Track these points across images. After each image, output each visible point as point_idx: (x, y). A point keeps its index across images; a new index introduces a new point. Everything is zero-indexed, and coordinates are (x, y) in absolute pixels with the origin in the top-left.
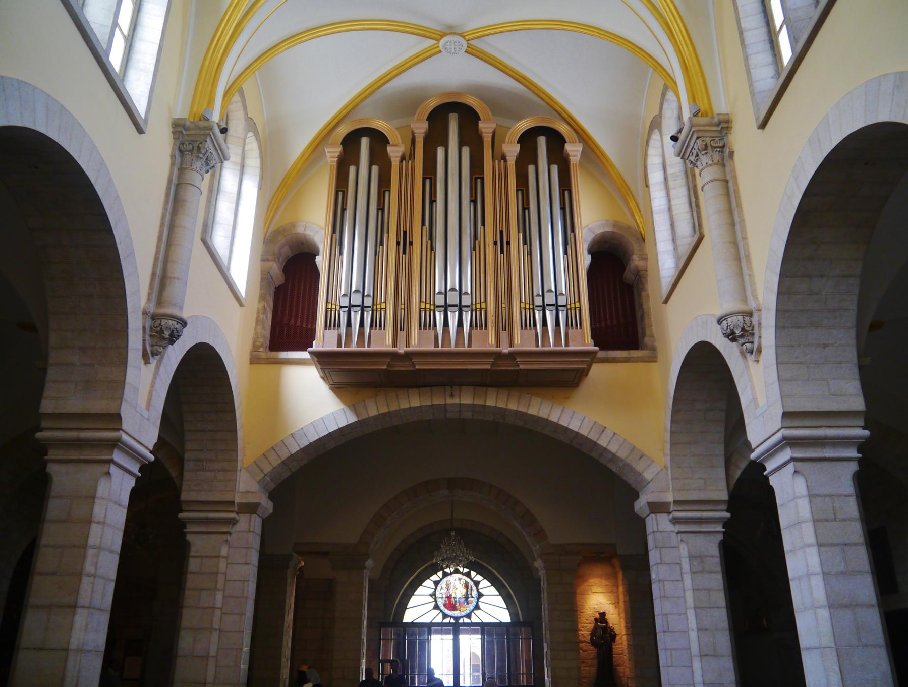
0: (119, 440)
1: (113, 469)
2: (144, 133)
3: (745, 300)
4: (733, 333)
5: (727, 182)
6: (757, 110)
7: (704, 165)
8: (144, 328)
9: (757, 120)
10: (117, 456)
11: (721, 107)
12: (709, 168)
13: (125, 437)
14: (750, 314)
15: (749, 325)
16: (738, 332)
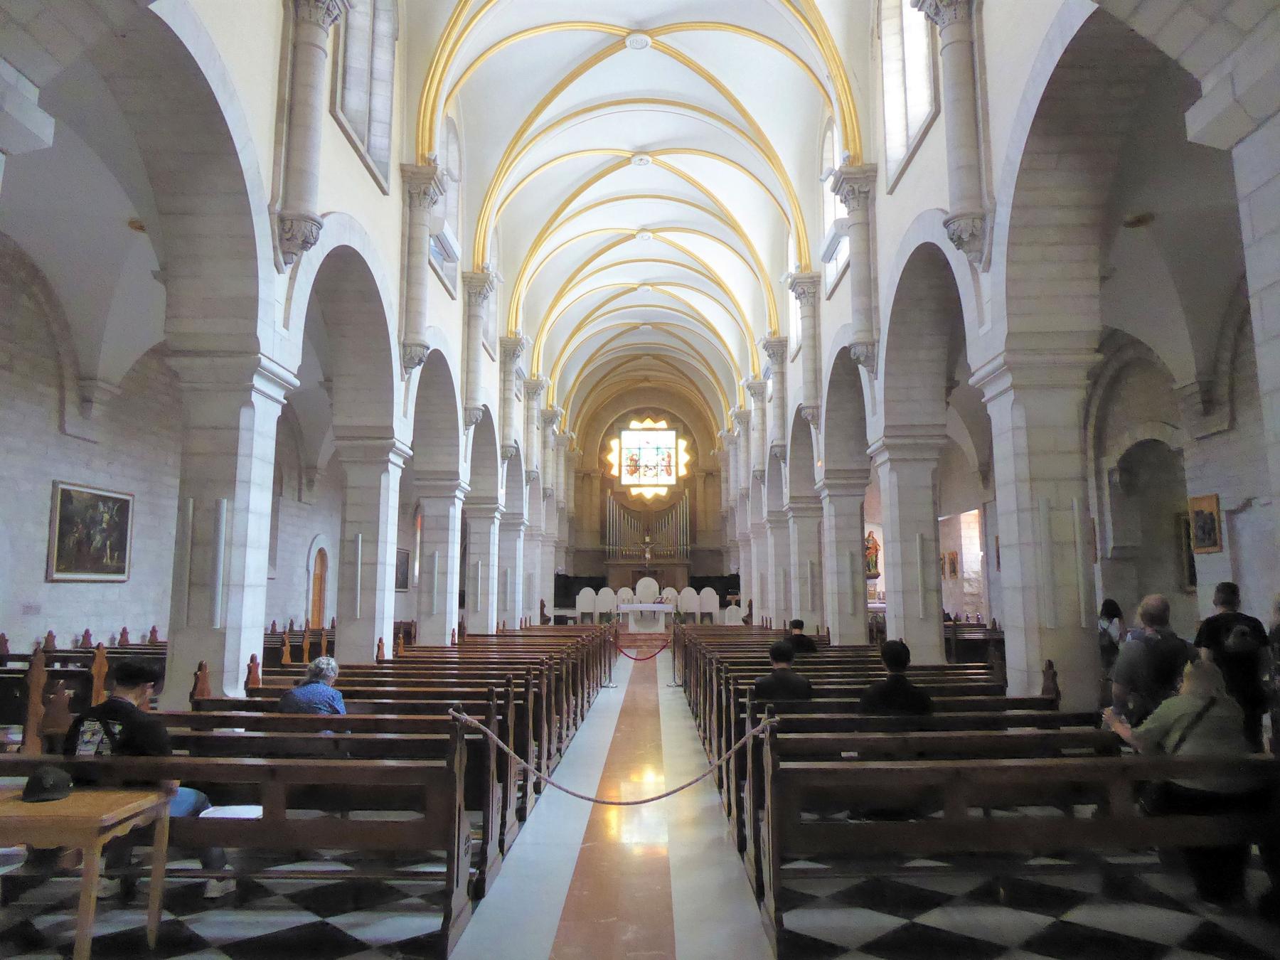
3: (870, 331)
5: (868, 224)
11: (867, 159)
16: (862, 359)
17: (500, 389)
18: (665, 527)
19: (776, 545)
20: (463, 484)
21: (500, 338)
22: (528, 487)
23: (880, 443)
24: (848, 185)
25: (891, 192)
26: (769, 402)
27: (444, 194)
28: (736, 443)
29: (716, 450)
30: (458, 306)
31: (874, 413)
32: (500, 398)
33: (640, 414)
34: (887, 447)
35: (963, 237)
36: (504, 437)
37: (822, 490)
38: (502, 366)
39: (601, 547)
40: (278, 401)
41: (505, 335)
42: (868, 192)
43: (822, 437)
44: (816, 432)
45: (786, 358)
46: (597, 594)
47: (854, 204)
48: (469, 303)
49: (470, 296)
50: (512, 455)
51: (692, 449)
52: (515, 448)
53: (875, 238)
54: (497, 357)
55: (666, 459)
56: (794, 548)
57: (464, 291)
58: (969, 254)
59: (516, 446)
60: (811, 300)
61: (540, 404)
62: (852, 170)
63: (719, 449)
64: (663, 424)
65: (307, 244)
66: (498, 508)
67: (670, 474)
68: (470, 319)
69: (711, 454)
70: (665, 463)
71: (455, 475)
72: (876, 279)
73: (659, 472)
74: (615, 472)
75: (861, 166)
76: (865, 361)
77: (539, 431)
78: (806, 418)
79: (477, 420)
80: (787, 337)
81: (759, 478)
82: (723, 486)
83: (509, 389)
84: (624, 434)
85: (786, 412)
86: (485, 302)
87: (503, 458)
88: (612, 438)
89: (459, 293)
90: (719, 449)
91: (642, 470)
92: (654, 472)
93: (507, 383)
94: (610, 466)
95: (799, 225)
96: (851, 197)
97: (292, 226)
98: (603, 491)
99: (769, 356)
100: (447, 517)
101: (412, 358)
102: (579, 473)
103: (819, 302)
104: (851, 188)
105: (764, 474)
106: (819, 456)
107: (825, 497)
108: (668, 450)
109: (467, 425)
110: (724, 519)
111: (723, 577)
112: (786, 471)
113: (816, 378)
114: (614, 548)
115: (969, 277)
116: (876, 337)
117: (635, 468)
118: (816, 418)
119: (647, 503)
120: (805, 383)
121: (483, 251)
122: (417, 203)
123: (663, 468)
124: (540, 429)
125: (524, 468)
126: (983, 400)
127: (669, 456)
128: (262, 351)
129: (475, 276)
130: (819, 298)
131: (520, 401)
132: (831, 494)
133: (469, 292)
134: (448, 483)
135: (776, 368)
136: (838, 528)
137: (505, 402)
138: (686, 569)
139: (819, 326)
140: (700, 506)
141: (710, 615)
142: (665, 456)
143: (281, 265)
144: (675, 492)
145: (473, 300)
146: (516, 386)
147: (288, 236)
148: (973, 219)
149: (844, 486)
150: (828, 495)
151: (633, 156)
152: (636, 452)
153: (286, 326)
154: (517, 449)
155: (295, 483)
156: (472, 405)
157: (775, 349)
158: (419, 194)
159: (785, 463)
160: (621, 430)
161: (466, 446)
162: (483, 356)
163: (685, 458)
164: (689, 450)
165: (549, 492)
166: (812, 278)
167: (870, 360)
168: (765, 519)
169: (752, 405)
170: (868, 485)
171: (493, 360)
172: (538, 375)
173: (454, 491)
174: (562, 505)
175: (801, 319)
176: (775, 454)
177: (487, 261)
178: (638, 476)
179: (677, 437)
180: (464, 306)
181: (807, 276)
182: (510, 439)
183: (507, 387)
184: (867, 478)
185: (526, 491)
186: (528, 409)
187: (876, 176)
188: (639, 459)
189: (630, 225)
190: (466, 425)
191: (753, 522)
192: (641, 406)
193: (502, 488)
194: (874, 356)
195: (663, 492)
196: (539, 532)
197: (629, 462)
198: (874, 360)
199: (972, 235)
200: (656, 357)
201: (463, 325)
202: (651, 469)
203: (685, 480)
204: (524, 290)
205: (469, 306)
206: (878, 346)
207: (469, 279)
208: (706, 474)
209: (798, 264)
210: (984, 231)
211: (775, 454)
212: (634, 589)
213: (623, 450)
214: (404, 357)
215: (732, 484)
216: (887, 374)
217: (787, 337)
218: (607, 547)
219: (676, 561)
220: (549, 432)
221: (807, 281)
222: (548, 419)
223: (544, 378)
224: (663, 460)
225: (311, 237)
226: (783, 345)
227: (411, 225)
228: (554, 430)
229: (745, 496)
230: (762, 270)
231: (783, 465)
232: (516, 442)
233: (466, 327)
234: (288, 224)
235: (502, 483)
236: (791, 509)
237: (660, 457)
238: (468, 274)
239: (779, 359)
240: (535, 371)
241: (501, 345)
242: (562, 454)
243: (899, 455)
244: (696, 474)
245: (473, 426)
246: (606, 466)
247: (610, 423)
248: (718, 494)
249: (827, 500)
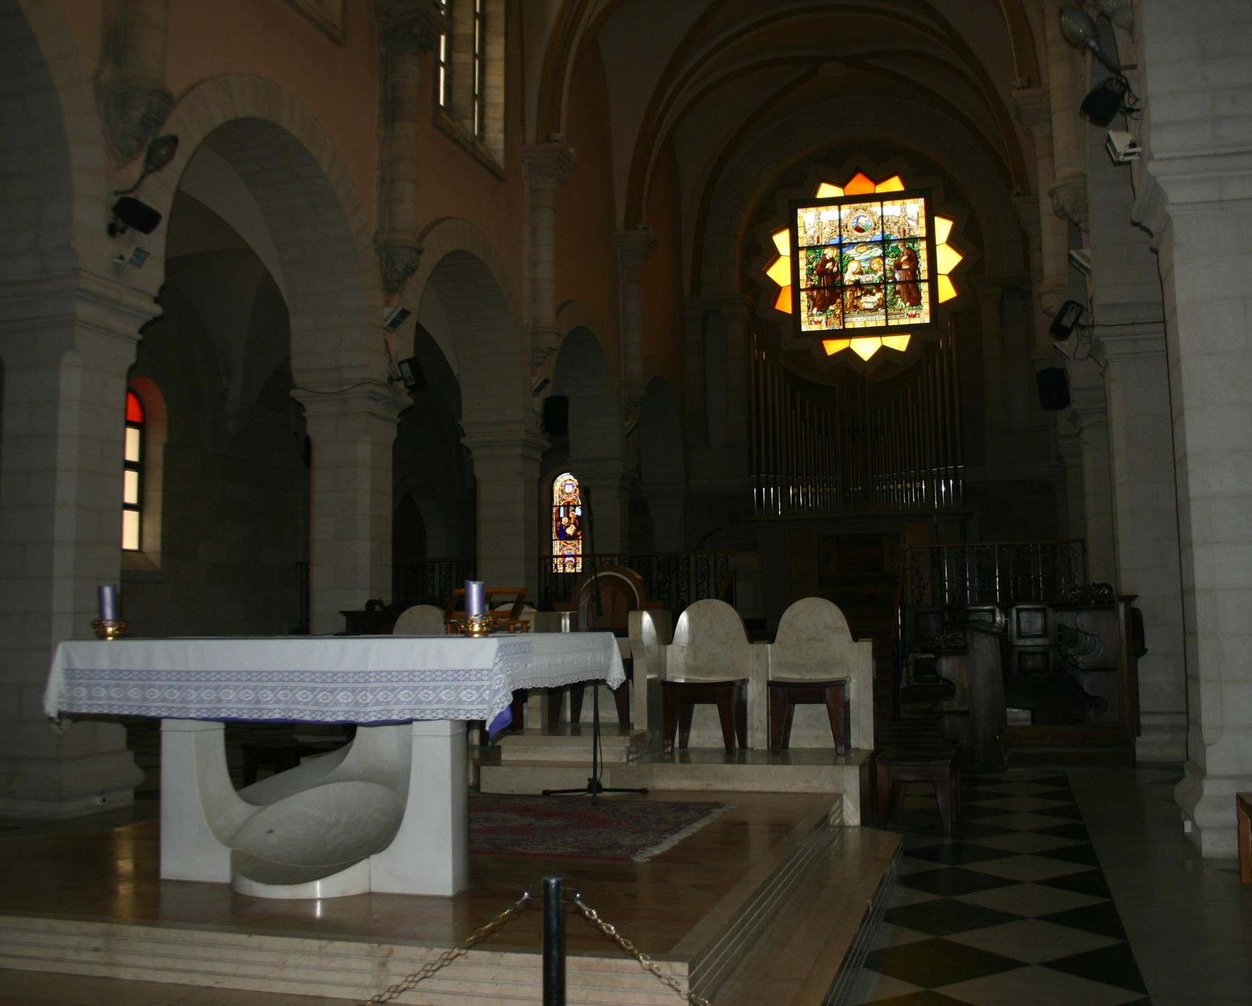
64: (895, 184)
73: (889, 298)
74: (784, 304)
123: (898, 287)
163: (948, 259)
164: (952, 241)
178: (838, 312)
188: (841, 273)
195: (900, 343)
197: (816, 278)
202: (871, 293)
213: (802, 254)
237: (890, 262)
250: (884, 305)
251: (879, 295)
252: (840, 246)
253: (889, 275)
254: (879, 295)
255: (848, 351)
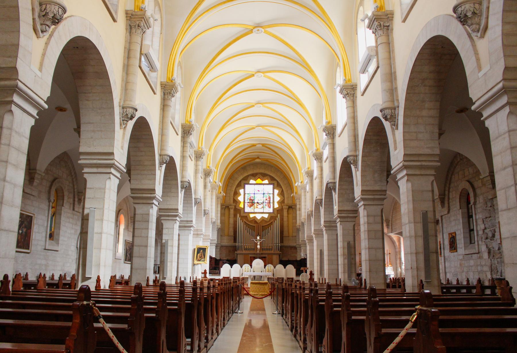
0: (114, 164)
1: (112, 176)
2: (117, 22)
3: (393, 101)
4: (386, 117)
5: (389, 44)
6: (402, 14)
7: (379, 35)
8: (120, 112)
9: (402, 17)
10: (113, 170)
11: (388, 8)
12: (381, 37)
13: (116, 163)
14: (395, 109)
15: (393, 113)
16: (388, 117)
17: (181, 151)
18: (267, 234)
19: (328, 240)
20: (157, 196)
21: (182, 124)
22: (196, 207)
23: (401, 164)
24: (377, 22)
25: (404, 21)
26: (325, 162)
27: (150, 28)
28: (305, 189)
29: (294, 194)
30: (158, 98)
31: (396, 149)
32: (181, 156)
33: (255, 176)
34: (405, 167)
35: (468, 14)
36: (182, 177)
37: (359, 202)
38: (182, 139)
39: (234, 244)
40: (32, 116)
41: (184, 123)
42: (389, 26)
43: (359, 173)
44: (355, 170)
45: (335, 136)
46: (231, 267)
47: (380, 32)
48: (164, 98)
49: (164, 94)
50: (186, 186)
51: (281, 194)
52: (188, 183)
53: (393, 51)
54: (180, 133)
55: (268, 200)
56: (340, 239)
57: (161, 92)
58: (471, 27)
59: (189, 181)
60: (352, 98)
61: (203, 164)
62: (380, 13)
63: (296, 193)
64: (266, 181)
65: (56, 21)
66: (178, 215)
67: (270, 207)
68: (164, 106)
69: (292, 196)
70: (267, 201)
71: (153, 191)
72: (395, 72)
73: (264, 206)
74: (241, 206)
75: (384, 12)
76: (390, 118)
77: (203, 179)
78: (350, 162)
79: (166, 161)
80: (336, 125)
81: (319, 203)
82: (298, 212)
83: (185, 151)
84: (247, 186)
85: (336, 164)
86: (173, 99)
87: (182, 188)
88: (241, 189)
89: (158, 90)
90: (296, 193)
91: (255, 205)
92: (262, 206)
93: (185, 148)
94: (240, 202)
95: (344, 58)
96: (379, 28)
97: (46, 7)
98: (235, 216)
99: (326, 135)
100: (148, 214)
101: (127, 115)
102: (223, 206)
103: (356, 99)
104: (379, 24)
105: (322, 201)
106: (357, 183)
107: (361, 206)
108: (269, 195)
109: (161, 164)
110: (298, 230)
111: (296, 261)
112: (335, 196)
113: (355, 139)
114: (242, 244)
115: (468, 43)
116: (396, 104)
117: (252, 203)
118: (355, 163)
119: (258, 222)
120: (349, 143)
121: (172, 71)
122: (134, 30)
123: (266, 204)
124: (203, 178)
125: (193, 196)
126: (482, 119)
127: (270, 198)
128: (19, 78)
129: (167, 84)
130: (356, 97)
131: (192, 160)
132: (365, 203)
133: (164, 93)
134: (149, 195)
135: (330, 141)
136: (368, 223)
137: (183, 157)
138: (278, 256)
139: (357, 112)
140: (285, 224)
141: (292, 279)
142: (268, 198)
143: (39, 31)
144: (272, 217)
145: (166, 97)
146: (190, 152)
147: (44, 13)
148: (474, 3)
149: (374, 199)
150: (363, 204)
151: (254, 28)
152: (253, 195)
153: (40, 70)
154: (189, 183)
155: (71, 200)
156: (164, 153)
157: (329, 131)
158: (135, 26)
159: (335, 192)
160: (245, 184)
161: (160, 176)
162: (171, 130)
163: (277, 199)
164: (278, 195)
165: (207, 212)
166: (352, 86)
167: (392, 118)
168: (323, 226)
169: (315, 165)
170: (385, 198)
171: (177, 135)
172: (202, 148)
173: (153, 200)
174: (214, 220)
175: (346, 108)
176: (330, 187)
177: (175, 76)
178: (253, 208)
179: (274, 189)
180: (161, 100)
181: (349, 85)
182: (185, 178)
183: (184, 150)
184: (385, 195)
185: (194, 209)
186: (196, 165)
187: (393, 17)
188: (254, 200)
189: (252, 69)
190: (160, 164)
191: (315, 229)
192: (255, 171)
193: (181, 204)
194: (395, 115)
195: (266, 216)
196: (201, 233)
197: (249, 201)
198: (396, 117)
199: (474, 13)
200: (263, 145)
201: (160, 110)
202: (260, 204)
203: (278, 211)
204: (195, 101)
205: (164, 100)
206: (398, 110)
207: (164, 86)
208: (289, 207)
209: (344, 78)
210: (481, 11)
211: (330, 187)
212: (251, 266)
213: (246, 195)
214: (122, 114)
215: (303, 210)
216: (405, 124)
217: (336, 125)
218: (237, 244)
219: (272, 252)
220: (208, 180)
221: (349, 87)
222: (207, 174)
223: (205, 150)
224: (266, 200)
225: (58, 15)
226: (333, 129)
227: (130, 43)
228: (210, 180)
229: (309, 216)
230: (322, 89)
231: (333, 193)
232: (189, 180)
233: (162, 110)
234: (44, 6)
235: (181, 202)
236: (339, 217)
237: (265, 198)
238: (164, 83)
239: (332, 136)
240: (200, 146)
241: (182, 127)
242: (214, 194)
243: (411, 172)
244: (283, 207)
245: (165, 164)
246: (237, 202)
247: (240, 179)
248: (295, 218)
249: (363, 207)
250: (263, 207)
251: (262, 205)
252: (254, 194)
253: (264, 201)
254: (262, 205)
255: (255, 217)
